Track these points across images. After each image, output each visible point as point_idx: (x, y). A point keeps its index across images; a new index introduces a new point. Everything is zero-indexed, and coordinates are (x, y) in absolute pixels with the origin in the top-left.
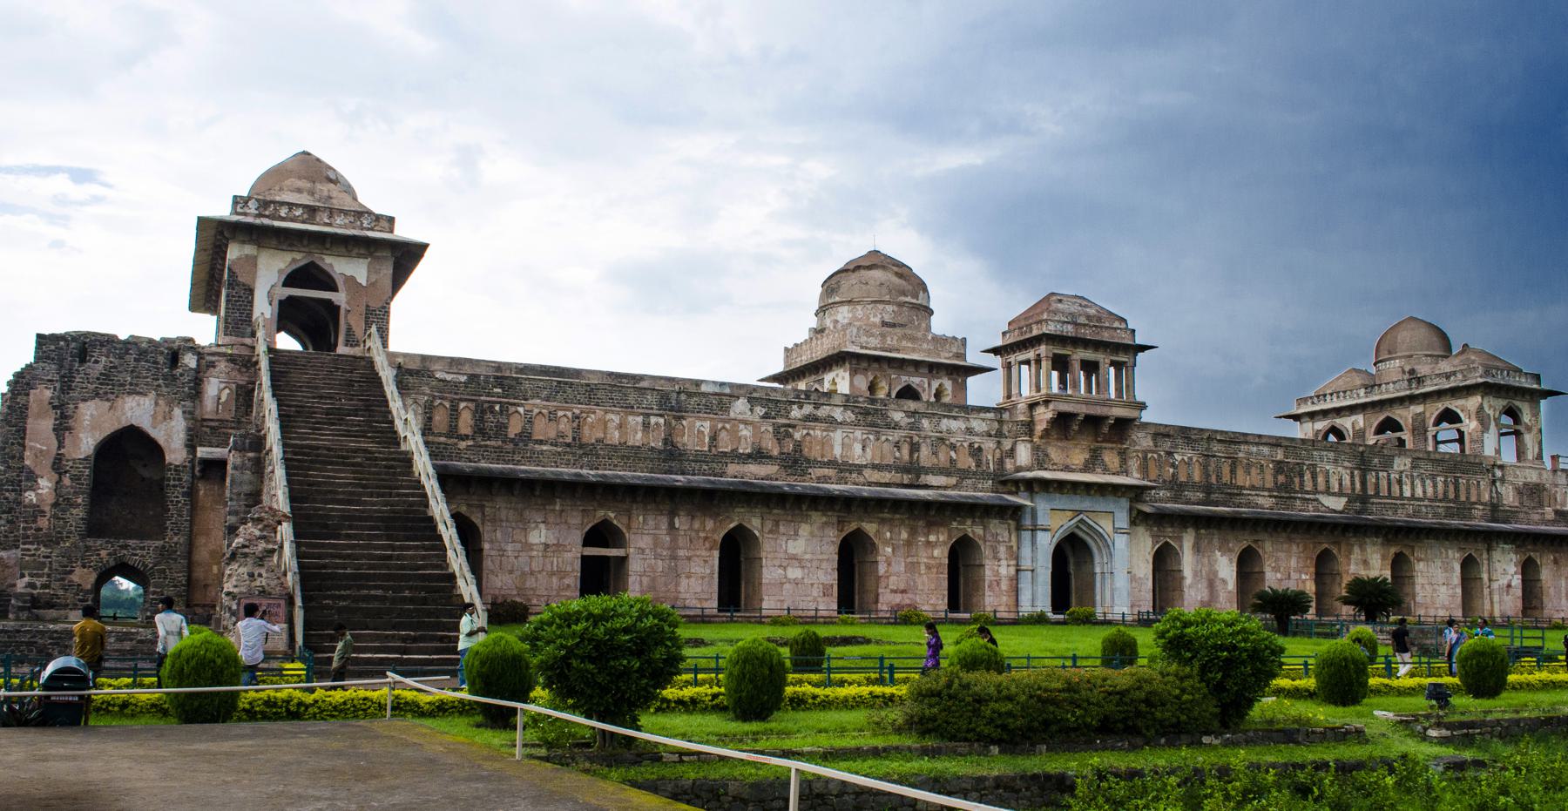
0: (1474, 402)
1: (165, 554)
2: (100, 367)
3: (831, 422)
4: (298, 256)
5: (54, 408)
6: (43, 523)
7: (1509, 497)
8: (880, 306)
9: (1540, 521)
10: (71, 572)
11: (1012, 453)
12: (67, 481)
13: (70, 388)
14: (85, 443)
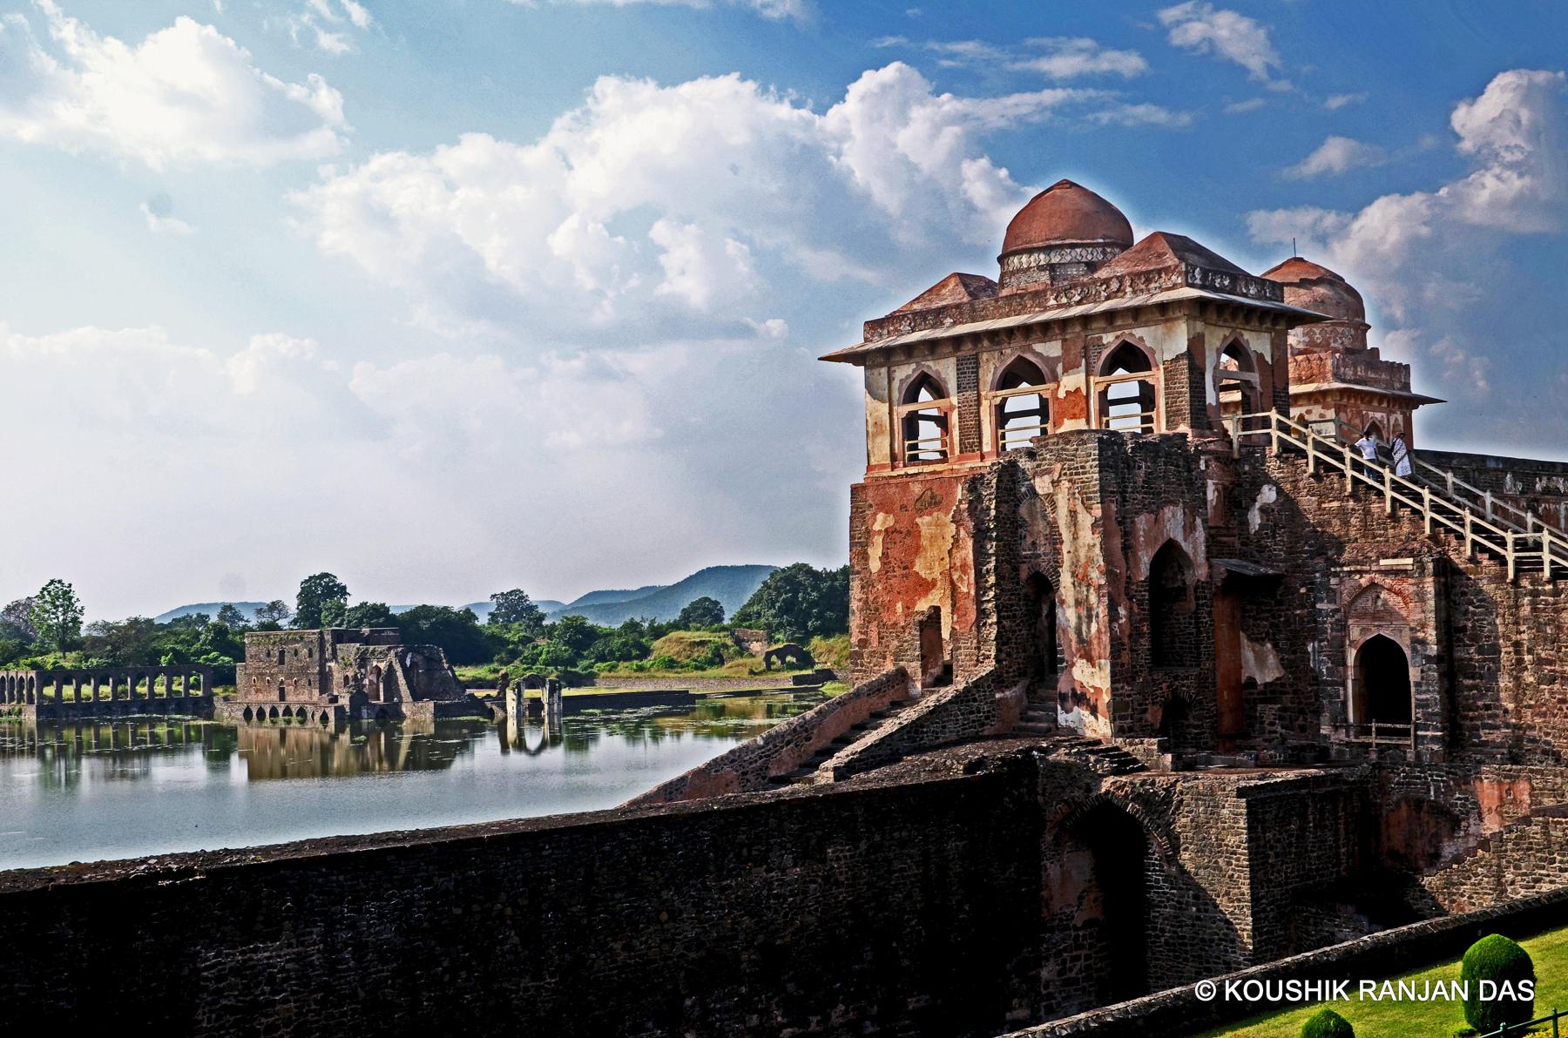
1: (1203, 682)
2: (1142, 472)
4: (1227, 332)
5: (1120, 523)
6: (1126, 657)
8: (1340, 330)
10: (1145, 711)
12: (1136, 610)
13: (1124, 500)
14: (1145, 558)
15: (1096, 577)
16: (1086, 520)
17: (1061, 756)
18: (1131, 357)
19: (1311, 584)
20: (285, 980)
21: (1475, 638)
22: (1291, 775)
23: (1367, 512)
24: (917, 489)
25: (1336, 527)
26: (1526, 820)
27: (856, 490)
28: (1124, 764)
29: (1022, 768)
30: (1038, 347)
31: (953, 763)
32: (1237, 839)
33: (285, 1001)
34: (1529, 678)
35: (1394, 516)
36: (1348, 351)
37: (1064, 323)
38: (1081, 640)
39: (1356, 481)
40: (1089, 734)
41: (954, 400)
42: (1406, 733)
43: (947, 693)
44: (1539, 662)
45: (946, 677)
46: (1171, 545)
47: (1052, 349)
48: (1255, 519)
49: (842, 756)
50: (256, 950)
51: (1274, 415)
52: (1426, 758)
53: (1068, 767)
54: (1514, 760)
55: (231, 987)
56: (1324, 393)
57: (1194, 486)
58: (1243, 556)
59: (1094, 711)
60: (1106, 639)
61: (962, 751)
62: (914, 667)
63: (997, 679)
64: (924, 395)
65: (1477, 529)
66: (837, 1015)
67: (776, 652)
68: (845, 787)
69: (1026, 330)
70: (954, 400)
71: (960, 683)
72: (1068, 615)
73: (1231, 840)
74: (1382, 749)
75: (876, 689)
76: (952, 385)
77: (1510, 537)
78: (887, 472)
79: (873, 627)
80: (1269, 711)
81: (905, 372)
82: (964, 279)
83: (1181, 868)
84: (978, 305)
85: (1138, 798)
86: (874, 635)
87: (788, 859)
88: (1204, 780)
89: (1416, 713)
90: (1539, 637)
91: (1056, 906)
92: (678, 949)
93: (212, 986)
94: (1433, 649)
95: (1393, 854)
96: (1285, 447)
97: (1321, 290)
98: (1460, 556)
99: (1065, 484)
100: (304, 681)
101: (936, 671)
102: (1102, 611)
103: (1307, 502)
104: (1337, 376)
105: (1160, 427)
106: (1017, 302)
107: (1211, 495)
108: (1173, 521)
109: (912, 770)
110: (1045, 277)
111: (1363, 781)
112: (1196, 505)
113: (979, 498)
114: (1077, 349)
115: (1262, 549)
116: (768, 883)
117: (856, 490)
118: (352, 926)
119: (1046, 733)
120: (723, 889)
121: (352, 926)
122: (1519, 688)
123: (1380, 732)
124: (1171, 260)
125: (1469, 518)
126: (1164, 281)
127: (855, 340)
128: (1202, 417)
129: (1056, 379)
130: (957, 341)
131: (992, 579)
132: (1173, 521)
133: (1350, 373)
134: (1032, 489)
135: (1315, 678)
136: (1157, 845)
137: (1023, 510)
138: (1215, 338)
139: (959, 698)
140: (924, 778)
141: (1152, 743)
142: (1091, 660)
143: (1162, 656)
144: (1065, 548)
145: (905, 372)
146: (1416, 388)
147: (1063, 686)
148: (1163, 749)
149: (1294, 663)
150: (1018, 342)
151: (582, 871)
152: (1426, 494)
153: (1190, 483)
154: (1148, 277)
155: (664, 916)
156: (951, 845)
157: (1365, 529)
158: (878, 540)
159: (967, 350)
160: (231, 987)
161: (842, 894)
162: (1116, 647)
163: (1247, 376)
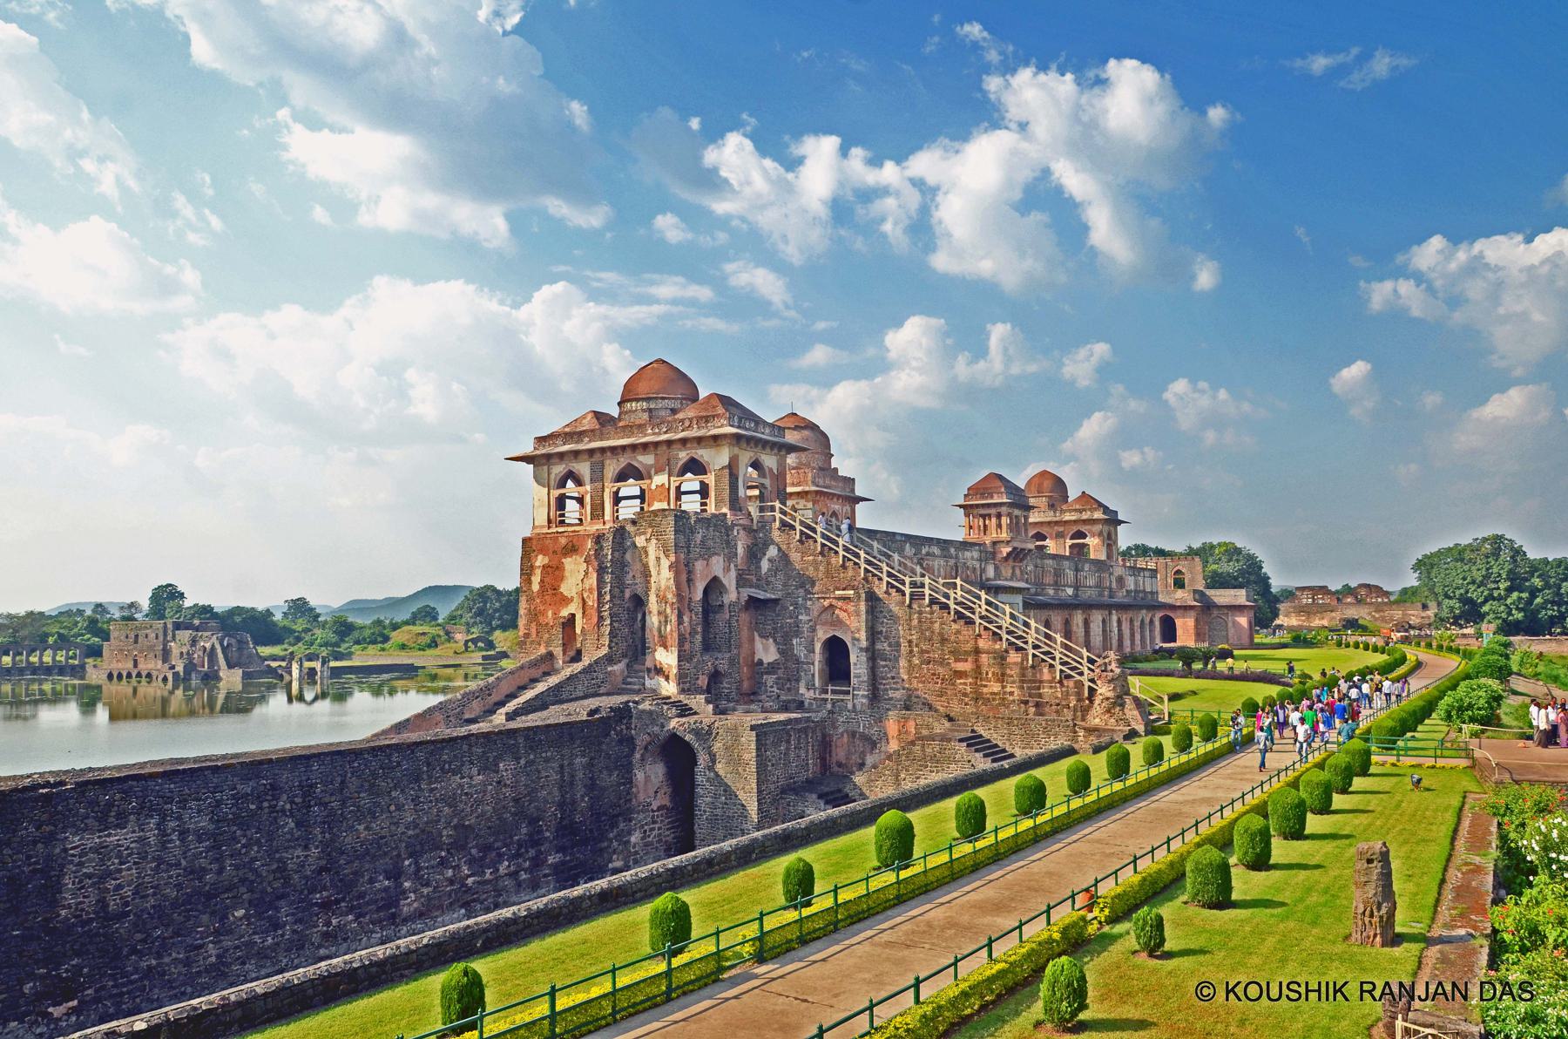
0: (1098, 527)
1: (732, 662)
3: (933, 555)
6: (687, 646)
7: (1114, 585)
9: (1121, 597)
11: (983, 571)
15: (670, 597)
16: (665, 563)
17: (646, 706)
18: (695, 466)
19: (796, 605)
20: (130, 855)
21: (887, 638)
22: (782, 717)
23: (829, 563)
24: (563, 541)
25: (811, 572)
26: (913, 743)
27: (525, 541)
28: (685, 711)
29: (623, 713)
30: (640, 458)
31: (579, 711)
32: (750, 755)
33: (129, 869)
34: (916, 661)
35: (843, 566)
36: (821, 469)
37: (656, 444)
38: (661, 636)
39: (823, 545)
40: (664, 693)
41: (588, 488)
42: (848, 693)
43: (578, 667)
44: (922, 652)
45: (577, 657)
46: (715, 579)
47: (646, 460)
48: (765, 565)
49: (511, 706)
50: (109, 835)
51: (777, 505)
52: (858, 708)
53: (650, 713)
54: (907, 708)
55: (90, 861)
56: (807, 493)
57: (730, 545)
58: (757, 587)
59: (667, 678)
60: (675, 635)
61: (586, 702)
62: (558, 651)
63: (609, 659)
64: (570, 484)
65: (890, 575)
66: (503, 868)
67: (472, 640)
68: (513, 725)
69: (634, 447)
70: (588, 488)
71: (586, 661)
72: (653, 620)
73: (746, 756)
74: (834, 702)
75: (534, 664)
76: (587, 479)
77: (907, 580)
78: (545, 530)
79: (533, 625)
80: (770, 680)
81: (559, 469)
82: (597, 415)
83: (717, 775)
84: (605, 430)
85: (692, 731)
86: (534, 631)
87: (475, 771)
88: (732, 719)
89: (853, 681)
90: (922, 637)
91: (641, 797)
92: (401, 829)
93: (76, 860)
94: (864, 644)
95: (840, 765)
96: (784, 524)
97: (806, 433)
98: (880, 589)
99: (654, 541)
100: (151, 655)
101: (572, 653)
102: (674, 618)
103: (795, 557)
104: (814, 483)
105: (711, 509)
106: (629, 429)
107: (740, 550)
108: (717, 565)
109: (554, 715)
110: (646, 416)
111: (823, 721)
112: (731, 556)
113: (602, 548)
114: (663, 460)
115: (768, 583)
116: (461, 786)
117: (525, 541)
118: (179, 818)
119: (638, 692)
120: (432, 790)
121: (179, 818)
122: (911, 667)
123: (834, 692)
124: (720, 410)
125: (885, 568)
126: (717, 422)
127: (528, 448)
128: (735, 503)
129: (650, 478)
130: (591, 452)
131: (608, 598)
132: (717, 565)
133: (821, 482)
134: (634, 544)
135: (798, 661)
136: (702, 759)
137: (628, 556)
138: (746, 457)
139: (585, 671)
140: (562, 720)
141: (701, 698)
142: (666, 647)
143: (707, 647)
144: (653, 580)
145: (559, 469)
146: (859, 492)
147: (649, 664)
148: (708, 702)
149: (785, 651)
150: (628, 454)
151: (339, 779)
152: (862, 554)
153: (728, 542)
154: (707, 419)
155: (393, 808)
156: (578, 760)
157: (828, 573)
158: (538, 572)
159: (597, 457)
160: (90, 861)
161: (507, 791)
162: (682, 641)
163: (763, 481)
